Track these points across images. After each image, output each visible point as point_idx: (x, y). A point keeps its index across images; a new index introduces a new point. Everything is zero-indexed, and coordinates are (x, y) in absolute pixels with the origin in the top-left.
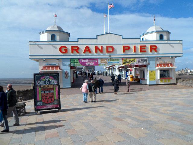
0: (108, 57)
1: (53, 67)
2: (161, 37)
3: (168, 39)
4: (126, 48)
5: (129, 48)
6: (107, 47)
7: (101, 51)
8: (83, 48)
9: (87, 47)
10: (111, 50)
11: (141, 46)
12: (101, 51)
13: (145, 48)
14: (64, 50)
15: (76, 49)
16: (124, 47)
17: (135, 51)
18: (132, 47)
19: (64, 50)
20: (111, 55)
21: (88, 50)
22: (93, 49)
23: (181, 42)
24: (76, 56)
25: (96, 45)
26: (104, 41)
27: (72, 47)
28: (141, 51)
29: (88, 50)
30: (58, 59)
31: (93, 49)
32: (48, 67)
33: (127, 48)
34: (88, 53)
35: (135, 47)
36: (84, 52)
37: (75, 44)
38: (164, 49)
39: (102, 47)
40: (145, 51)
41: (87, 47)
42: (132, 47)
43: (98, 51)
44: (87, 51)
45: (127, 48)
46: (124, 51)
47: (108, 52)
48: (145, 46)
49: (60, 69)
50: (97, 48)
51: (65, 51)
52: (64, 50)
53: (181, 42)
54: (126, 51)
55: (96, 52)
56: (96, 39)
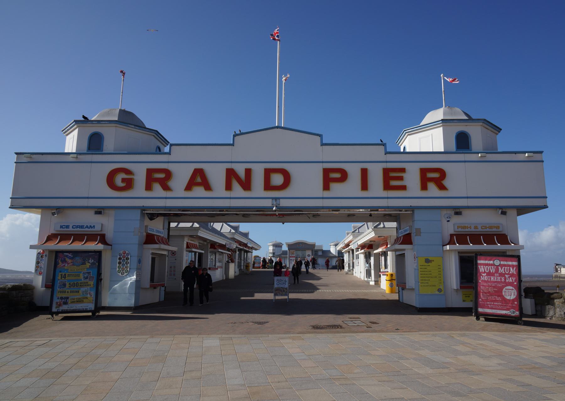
0: (267, 203)
2: (462, 142)
3: (491, 149)
4: (332, 176)
5: (344, 176)
6: (268, 173)
7: (246, 185)
8: (182, 175)
10: (277, 179)
11: (386, 172)
12: (246, 185)
13: (401, 178)
14: (123, 180)
15: (160, 178)
16: (326, 172)
17: (365, 186)
18: (354, 172)
20: (279, 198)
21: (199, 179)
22: (217, 176)
23: (537, 157)
24: (158, 198)
25: (229, 166)
26: (255, 153)
27: (150, 172)
28: (387, 187)
29: (199, 179)
30: (99, 211)
31: (217, 176)
32: (64, 237)
33: (338, 175)
34: (199, 191)
35: (364, 172)
36: (188, 188)
37: (156, 161)
38: (468, 181)
39: (248, 172)
40: (404, 188)
42: (354, 172)
43: (236, 185)
44: (198, 184)
45: (338, 175)
46: (326, 187)
47: (268, 186)
48: (403, 170)
50: (231, 174)
51: (123, 185)
52: (123, 180)
53: (537, 157)
54: (334, 186)
55: (229, 187)
56: (233, 145)
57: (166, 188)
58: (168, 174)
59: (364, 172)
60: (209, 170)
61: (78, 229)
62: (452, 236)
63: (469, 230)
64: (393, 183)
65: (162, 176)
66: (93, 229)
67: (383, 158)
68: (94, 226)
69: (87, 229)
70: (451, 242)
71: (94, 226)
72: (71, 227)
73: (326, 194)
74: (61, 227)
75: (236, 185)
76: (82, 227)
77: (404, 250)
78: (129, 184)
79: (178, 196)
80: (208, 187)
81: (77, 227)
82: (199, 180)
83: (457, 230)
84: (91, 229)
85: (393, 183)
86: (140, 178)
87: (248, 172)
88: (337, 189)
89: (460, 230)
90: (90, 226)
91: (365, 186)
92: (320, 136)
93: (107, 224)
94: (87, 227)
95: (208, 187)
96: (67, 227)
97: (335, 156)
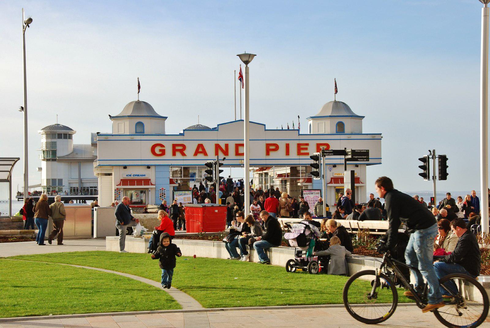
1: (139, 182)
5: (277, 148)
9: (200, 146)
11: (299, 145)
12: (226, 153)
13: (306, 149)
14: (160, 150)
16: (268, 145)
17: (288, 153)
19: (157, 150)
21: (200, 150)
22: (210, 148)
23: (377, 137)
24: (180, 160)
25: (216, 142)
27: (174, 146)
28: (299, 153)
29: (200, 150)
31: (210, 148)
33: (273, 147)
34: (200, 156)
35: (287, 146)
36: (196, 154)
39: (227, 146)
41: (200, 146)
43: (220, 153)
44: (201, 152)
45: (273, 147)
46: (268, 154)
48: (307, 144)
49: (152, 184)
50: (218, 147)
52: (160, 150)
53: (377, 137)
57: (184, 154)
58: (184, 147)
59: (287, 146)
60: (205, 144)
61: (136, 177)
62: (332, 178)
63: (341, 175)
64: (302, 151)
65: (181, 148)
66: (144, 177)
67: (298, 137)
68: (145, 175)
69: (141, 177)
70: (331, 182)
71: (145, 175)
72: (132, 176)
73: (268, 157)
74: (127, 176)
75: (220, 153)
76: (138, 175)
77: (308, 185)
78: (163, 152)
79: (189, 158)
80: (206, 154)
81: (136, 175)
82: (200, 150)
83: (334, 175)
84: (143, 177)
85: (302, 151)
86: (169, 150)
87: (227, 146)
88: (273, 154)
89: (336, 175)
90: (143, 175)
91: (288, 153)
92: (265, 125)
93: (150, 174)
94: (141, 175)
95: (206, 154)
96: (130, 175)
97: (272, 138)
